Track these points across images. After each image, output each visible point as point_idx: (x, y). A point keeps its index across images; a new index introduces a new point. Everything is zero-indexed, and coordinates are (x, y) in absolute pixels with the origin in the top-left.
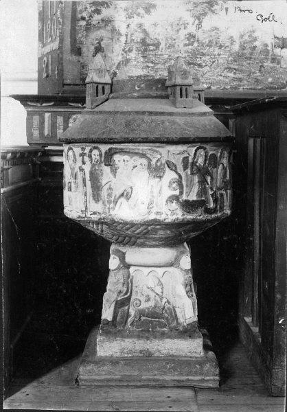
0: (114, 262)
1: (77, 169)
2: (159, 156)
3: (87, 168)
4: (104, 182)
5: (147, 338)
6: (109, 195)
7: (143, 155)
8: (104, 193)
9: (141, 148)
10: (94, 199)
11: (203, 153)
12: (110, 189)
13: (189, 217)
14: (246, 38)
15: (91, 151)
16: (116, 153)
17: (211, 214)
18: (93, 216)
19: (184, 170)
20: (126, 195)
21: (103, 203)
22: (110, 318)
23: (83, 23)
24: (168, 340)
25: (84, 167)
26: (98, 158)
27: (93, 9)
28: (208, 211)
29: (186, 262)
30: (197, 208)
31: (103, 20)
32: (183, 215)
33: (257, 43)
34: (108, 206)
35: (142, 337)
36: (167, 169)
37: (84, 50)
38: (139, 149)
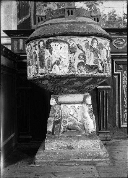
0: (53, 102)
1: (32, 54)
2: (73, 42)
3: (37, 52)
4: (46, 57)
5: (71, 140)
6: (49, 64)
7: (65, 42)
8: (46, 63)
9: (64, 38)
10: (41, 67)
12: (49, 60)
13: (90, 74)
14: (111, 15)
15: (39, 43)
16: (51, 42)
17: (101, 73)
18: (41, 76)
19: (86, 49)
20: (58, 63)
21: (46, 68)
22: (51, 131)
24: (81, 141)
25: (36, 51)
26: (43, 45)
28: (100, 71)
29: (89, 100)
30: (94, 69)
31: (47, 9)
32: (87, 72)
33: (116, 17)
34: (48, 69)
35: (68, 140)
36: (78, 49)
38: (63, 39)
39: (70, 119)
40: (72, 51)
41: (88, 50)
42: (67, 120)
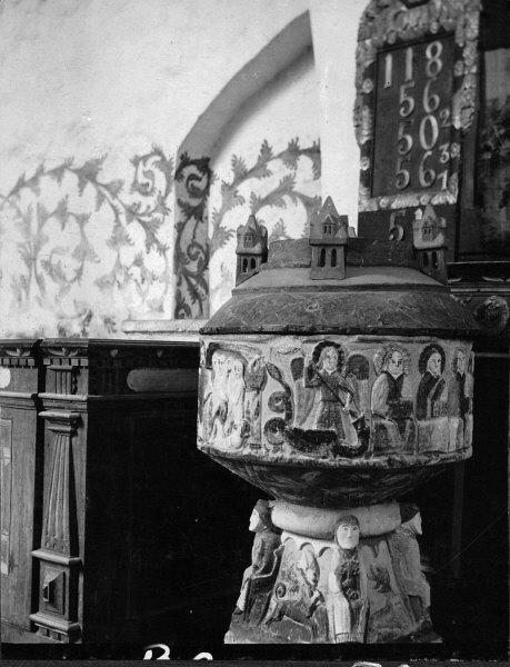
7: (238, 355)
9: (236, 343)
11: (436, 356)
13: (302, 457)
19: (295, 379)
23: (488, 156)
27: (502, 132)
30: (319, 444)
32: (293, 453)
37: (488, 196)
39: (296, 582)
40: (255, 383)
41: (303, 381)
42: (288, 585)
